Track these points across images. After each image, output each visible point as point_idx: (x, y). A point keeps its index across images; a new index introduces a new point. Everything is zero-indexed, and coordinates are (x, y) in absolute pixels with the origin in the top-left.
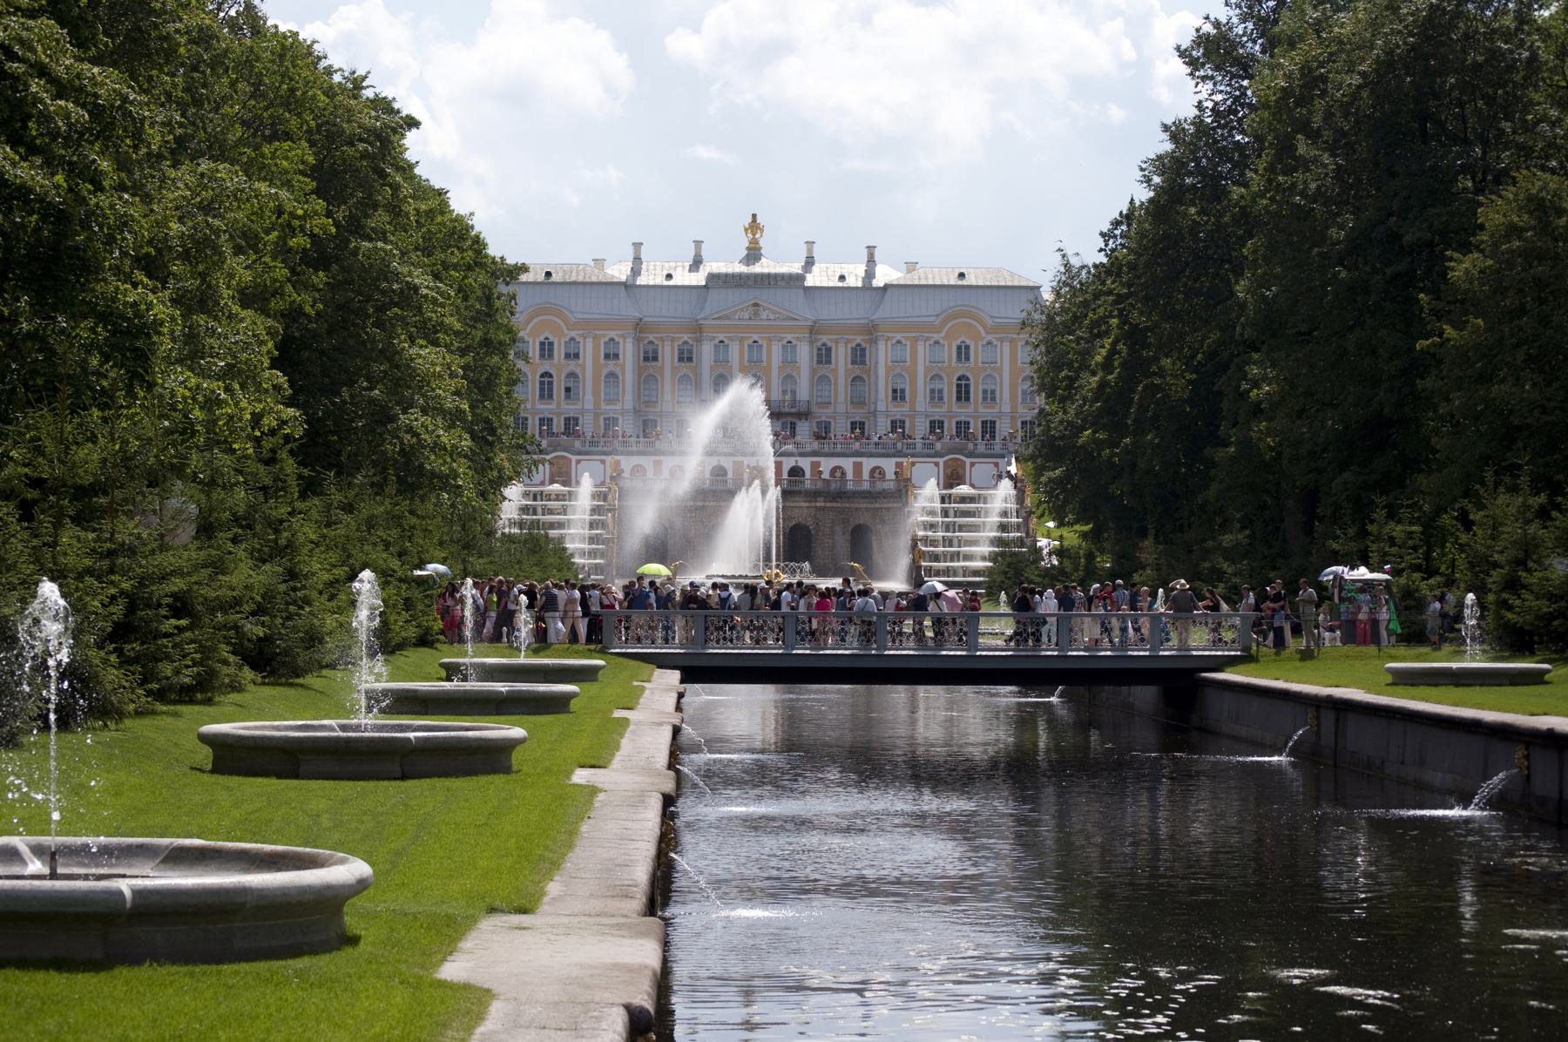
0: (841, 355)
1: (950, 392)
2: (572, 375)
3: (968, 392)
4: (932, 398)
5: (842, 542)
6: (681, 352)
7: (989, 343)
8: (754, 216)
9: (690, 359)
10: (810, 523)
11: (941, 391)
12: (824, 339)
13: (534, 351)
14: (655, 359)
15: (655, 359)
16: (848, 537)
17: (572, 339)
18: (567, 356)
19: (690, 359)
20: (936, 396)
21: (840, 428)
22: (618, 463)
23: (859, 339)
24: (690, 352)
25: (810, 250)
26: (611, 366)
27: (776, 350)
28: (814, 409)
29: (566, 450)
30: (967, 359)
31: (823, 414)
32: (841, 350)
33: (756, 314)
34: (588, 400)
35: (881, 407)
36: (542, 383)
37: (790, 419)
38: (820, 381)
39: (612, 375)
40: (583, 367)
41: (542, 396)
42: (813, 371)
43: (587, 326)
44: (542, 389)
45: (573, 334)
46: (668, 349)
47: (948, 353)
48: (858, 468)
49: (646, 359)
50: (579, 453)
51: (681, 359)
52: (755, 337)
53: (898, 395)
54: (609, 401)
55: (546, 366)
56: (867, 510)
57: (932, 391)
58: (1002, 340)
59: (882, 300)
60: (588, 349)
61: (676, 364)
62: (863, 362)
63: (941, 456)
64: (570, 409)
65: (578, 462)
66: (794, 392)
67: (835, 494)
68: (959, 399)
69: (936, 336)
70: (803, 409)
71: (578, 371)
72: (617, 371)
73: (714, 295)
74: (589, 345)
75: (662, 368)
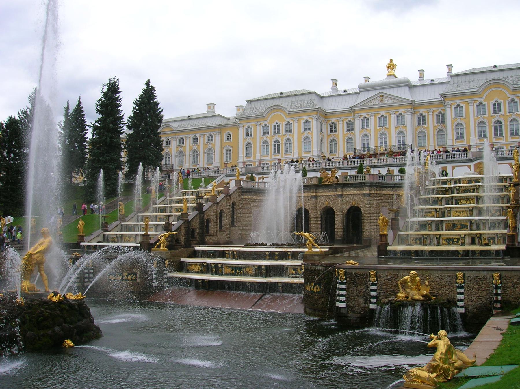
0: (431, 119)
1: (490, 131)
2: (288, 140)
3: (501, 130)
7: (513, 100)
8: (391, 61)
9: (352, 130)
10: (361, 205)
12: (421, 111)
13: (271, 130)
15: (335, 131)
17: (288, 122)
18: (287, 131)
19: (352, 130)
23: (440, 110)
25: (420, 74)
26: (306, 134)
32: (431, 117)
36: (275, 146)
39: (307, 138)
40: (293, 135)
41: (275, 152)
44: (275, 149)
45: (288, 120)
49: (331, 131)
51: (348, 130)
52: (382, 113)
53: (460, 137)
54: (305, 152)
55: (276, 137)
57: (480, 132)
60: (295, 127)
61: (345, 133)
63: (471, 161)
68: (496, 134)
71: (291, 138)
73: (362, 94)
74: (296, 125)
75: (338, 135)
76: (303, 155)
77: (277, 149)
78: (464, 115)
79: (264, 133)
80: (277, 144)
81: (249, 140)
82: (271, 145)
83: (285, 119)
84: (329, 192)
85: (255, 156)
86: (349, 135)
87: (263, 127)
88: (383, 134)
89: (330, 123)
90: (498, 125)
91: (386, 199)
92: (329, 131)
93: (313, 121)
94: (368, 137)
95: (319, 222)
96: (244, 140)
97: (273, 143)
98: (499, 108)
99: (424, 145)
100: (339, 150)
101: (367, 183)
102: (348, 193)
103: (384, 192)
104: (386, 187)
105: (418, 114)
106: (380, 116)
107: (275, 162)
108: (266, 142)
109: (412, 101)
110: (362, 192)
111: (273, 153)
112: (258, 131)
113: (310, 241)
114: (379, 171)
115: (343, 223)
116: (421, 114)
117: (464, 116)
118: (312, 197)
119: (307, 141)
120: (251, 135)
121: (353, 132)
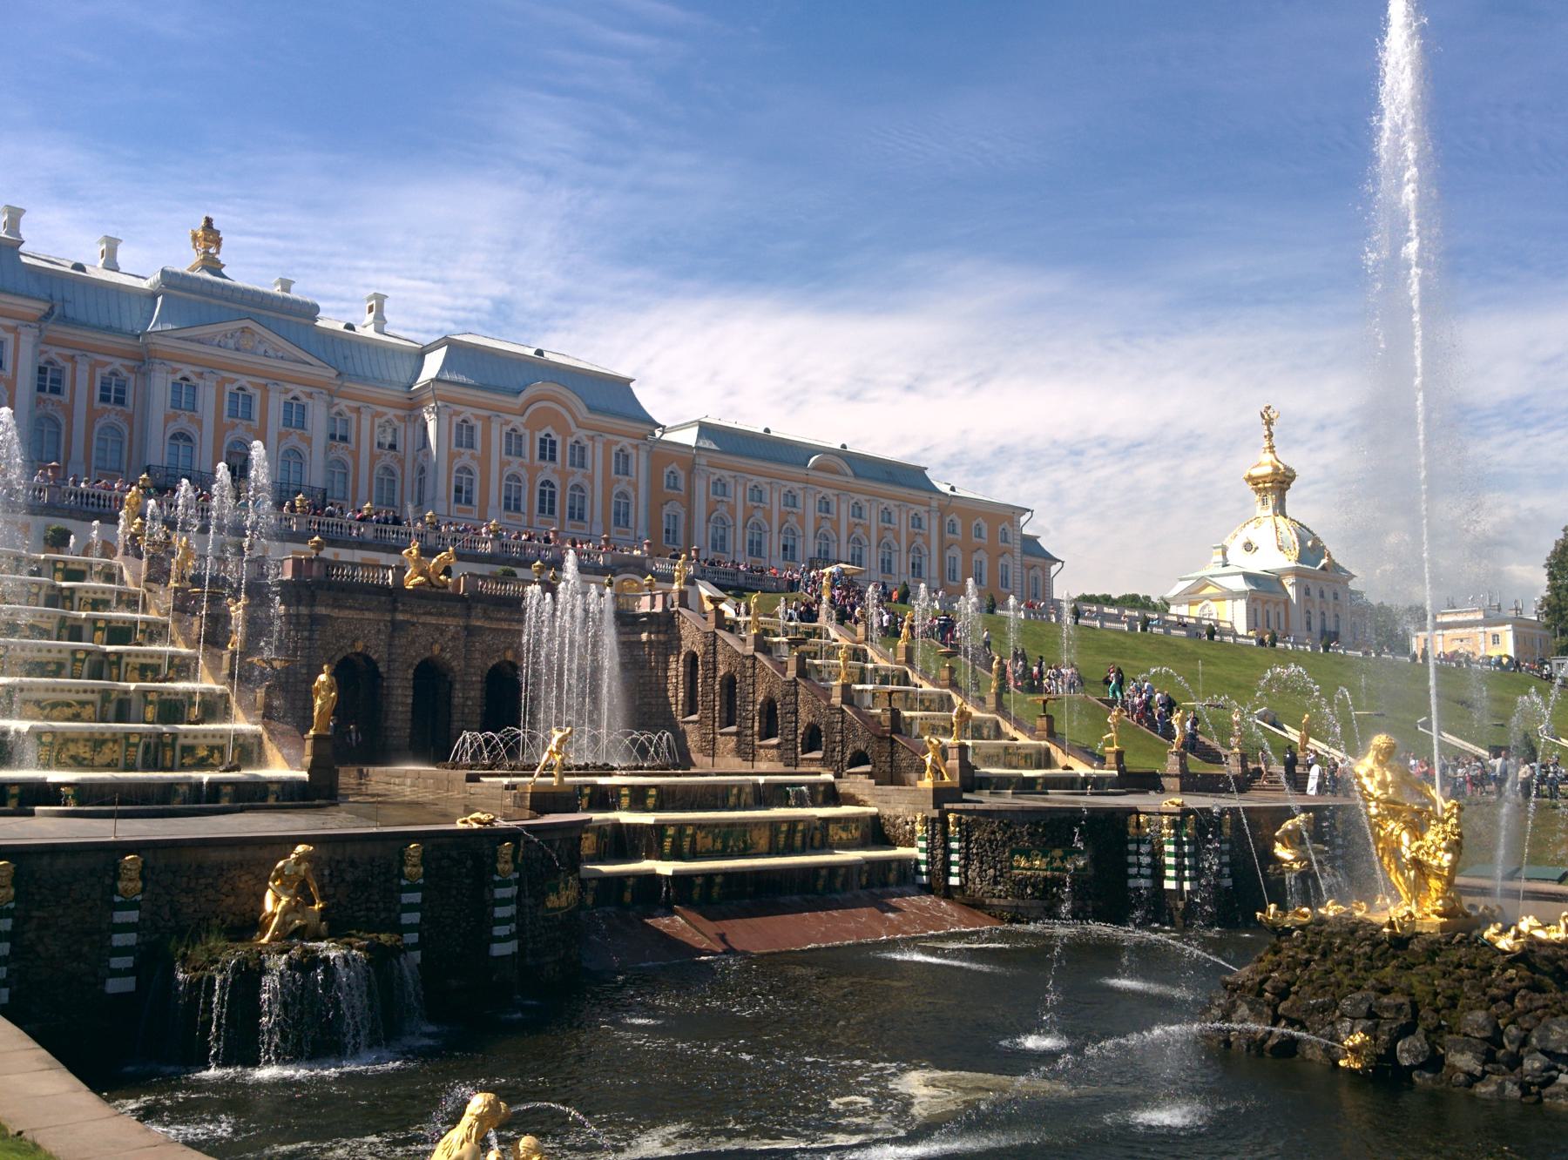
1: (530, 499)
3: (552, 502)
4: (507, 507)
6: (105, 388)
8: (209, 221)
9: (120, 401)
11: (518, 500)
12: (343, 404)
14: (56, 390)
15: (56, 390)
20: (512, 504)
24: (121, 391)
30: (553, 458)
38: (338, 468)
47: (531, 448)
49: (41, 389)
52: (244, 381)
57: (507, 498)
58: (592, 438)
61: (98, 405)
68: (542, 510)
69: (517, 421)
75: (69, 411)
84: (441, 614)
90: (547, 489)
93: (17, 340)
94: (189, 439)
95: (410, 701)
98: (553, 451)
105: (335, 410)
118: (396, 626)
121: (129, 410)
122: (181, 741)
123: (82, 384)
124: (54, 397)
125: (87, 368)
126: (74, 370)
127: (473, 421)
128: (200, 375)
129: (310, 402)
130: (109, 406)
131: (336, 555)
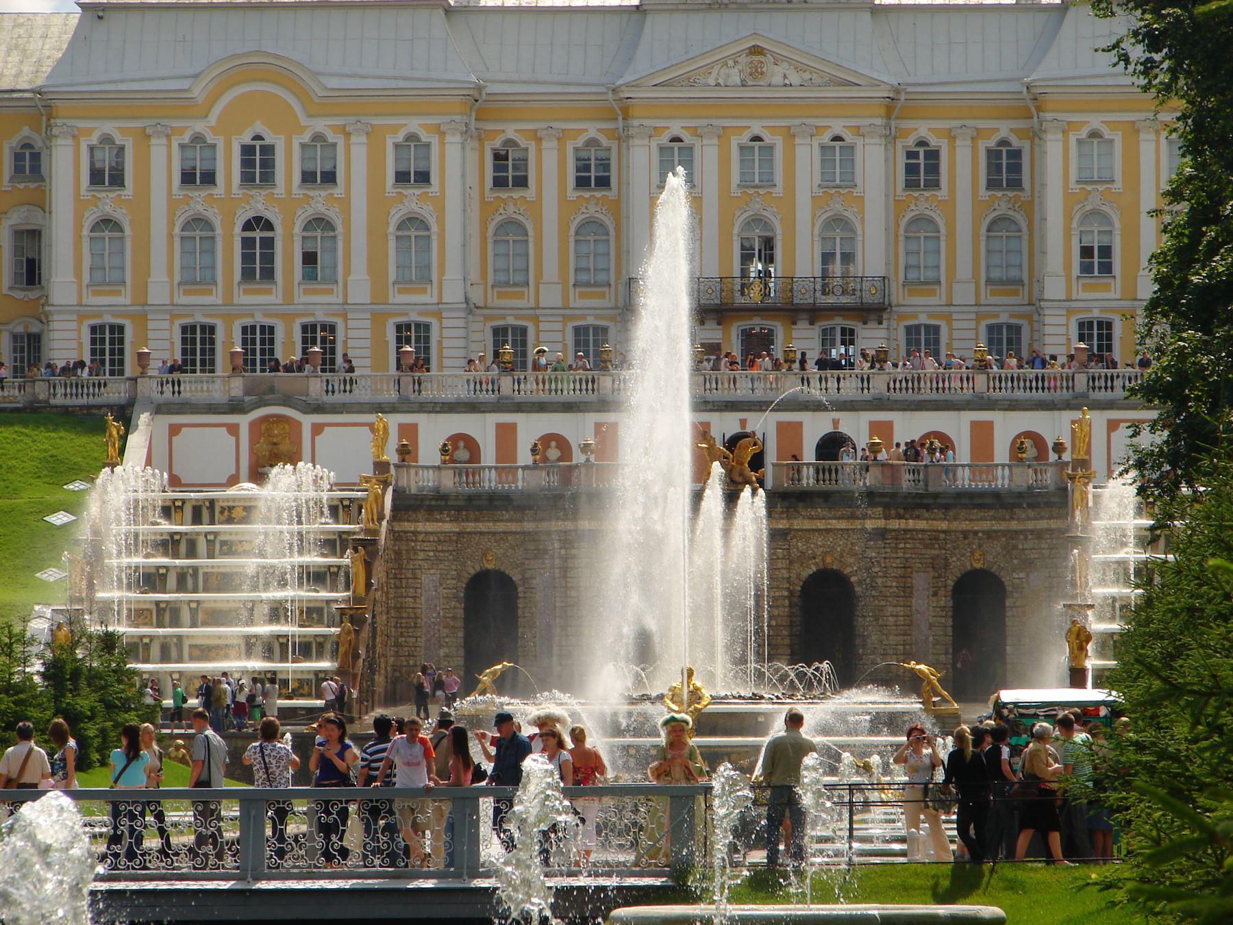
0: (963, 168)
2: (320, 223)
5: (930, 608)
9: (604, 182)
10: (852, 569)
12: (923, 129)
13: (229, 168)
14: (522, 182)
15: (522, 182)
16: (945, 601)
17: (318, 138)
18: (308, 177)
19: (604, 182)
21: (965, 338)
22: (409, 431)
23: (1004, 129)
24: (605, 165)
26: (413, 200)
27: (807, 157)
28: (898, 295)
29: (286, 401)
31: (919, 308)
33: (757, 73)
34: (357, 284)
35: (1054, 288)
36: (248, 243)
37: (839, 322)
39: (412, 221)
40: (345, 203)
41: (248, 274)
42: (898, 206)
43: (356, 104)
44: (247, 258)
45: (321, 125)
46: (550, 159)
48: (982, 436)
49: (499, 183)
50: (319, 409)
51: (582, 183)
52: (756, 127)
54: (404, 284)
55: (259, 203)
56: (989, 534)
59: (1054, 34)
60: (356, 163)
61: (572, 193)
62: (1016, 184)
64: (317, 304)
65: (317, 429)
66: (848, 258)
67: (916, 494)
70: (871, 296)
71: (333, 214)
72: (427, 211)
75: (537, 205)
76: (396, 298)
77: (258, 261)
78: (1118, 174)
79: (188, 178)
80: (258, 234)
81: (108, 202)
82: (229, 237)
83: (303, 121)
85: (142, 288)
86: (592, 209)
87: (183, 147)
88: (757, 220)
89: (497, 143)
91: (926, 547)
92: (489, 182)
93: (442, 144)
96: (80, 206)
97: (238, 229)
99: (931, 274)
100: (539, 275)
101: (882, 495)
102: (807, 525)
103: (922, 525)
104: (928, 508)
105: (910, 141)
106: (745, 139)
107: (248, 321)
108: (198, 222)
109: (897, 92)
110: (857, 524)
111: (237, 275)
112: (160, 166)
113: (930, 682)
114: (836, 423)
115: (791, 625)
116: (922, 143)
117: (1118, 185)
119: (413, 233)
120: (117, 179)
121: (612, 194)
122: (280, 676)
123: (551, 170)
124: (517, 194)
125: (554, 144)
126: (539, 151)
127: (1107, 134)
128: (694, 131)
129: (859, 142)
130: (587, 195)
131: (743, 423)
